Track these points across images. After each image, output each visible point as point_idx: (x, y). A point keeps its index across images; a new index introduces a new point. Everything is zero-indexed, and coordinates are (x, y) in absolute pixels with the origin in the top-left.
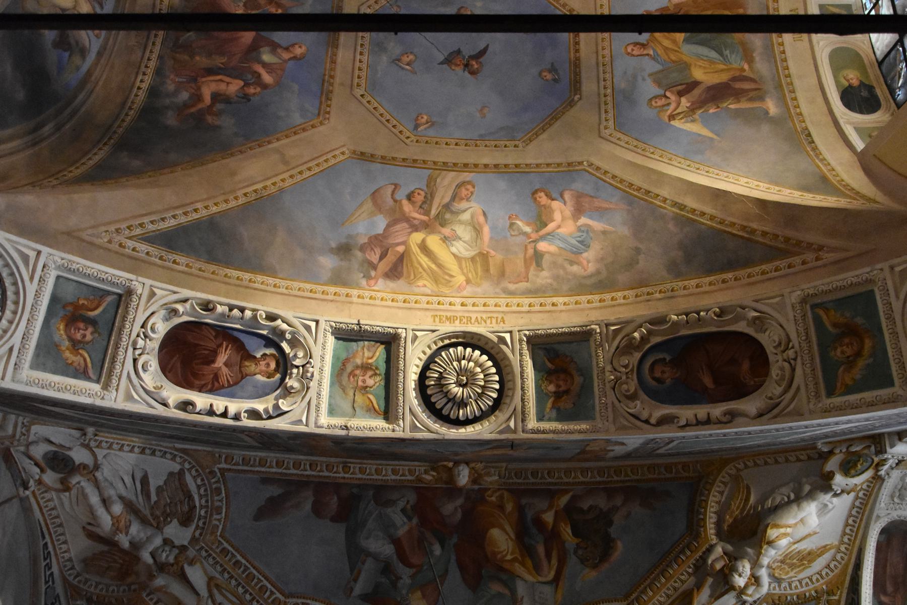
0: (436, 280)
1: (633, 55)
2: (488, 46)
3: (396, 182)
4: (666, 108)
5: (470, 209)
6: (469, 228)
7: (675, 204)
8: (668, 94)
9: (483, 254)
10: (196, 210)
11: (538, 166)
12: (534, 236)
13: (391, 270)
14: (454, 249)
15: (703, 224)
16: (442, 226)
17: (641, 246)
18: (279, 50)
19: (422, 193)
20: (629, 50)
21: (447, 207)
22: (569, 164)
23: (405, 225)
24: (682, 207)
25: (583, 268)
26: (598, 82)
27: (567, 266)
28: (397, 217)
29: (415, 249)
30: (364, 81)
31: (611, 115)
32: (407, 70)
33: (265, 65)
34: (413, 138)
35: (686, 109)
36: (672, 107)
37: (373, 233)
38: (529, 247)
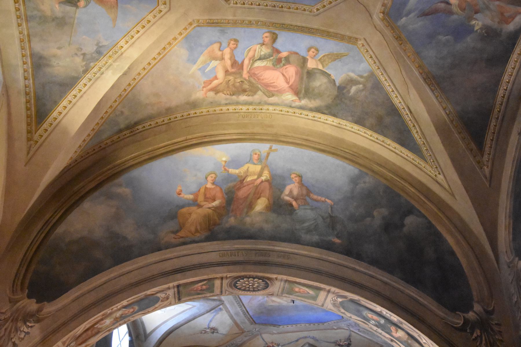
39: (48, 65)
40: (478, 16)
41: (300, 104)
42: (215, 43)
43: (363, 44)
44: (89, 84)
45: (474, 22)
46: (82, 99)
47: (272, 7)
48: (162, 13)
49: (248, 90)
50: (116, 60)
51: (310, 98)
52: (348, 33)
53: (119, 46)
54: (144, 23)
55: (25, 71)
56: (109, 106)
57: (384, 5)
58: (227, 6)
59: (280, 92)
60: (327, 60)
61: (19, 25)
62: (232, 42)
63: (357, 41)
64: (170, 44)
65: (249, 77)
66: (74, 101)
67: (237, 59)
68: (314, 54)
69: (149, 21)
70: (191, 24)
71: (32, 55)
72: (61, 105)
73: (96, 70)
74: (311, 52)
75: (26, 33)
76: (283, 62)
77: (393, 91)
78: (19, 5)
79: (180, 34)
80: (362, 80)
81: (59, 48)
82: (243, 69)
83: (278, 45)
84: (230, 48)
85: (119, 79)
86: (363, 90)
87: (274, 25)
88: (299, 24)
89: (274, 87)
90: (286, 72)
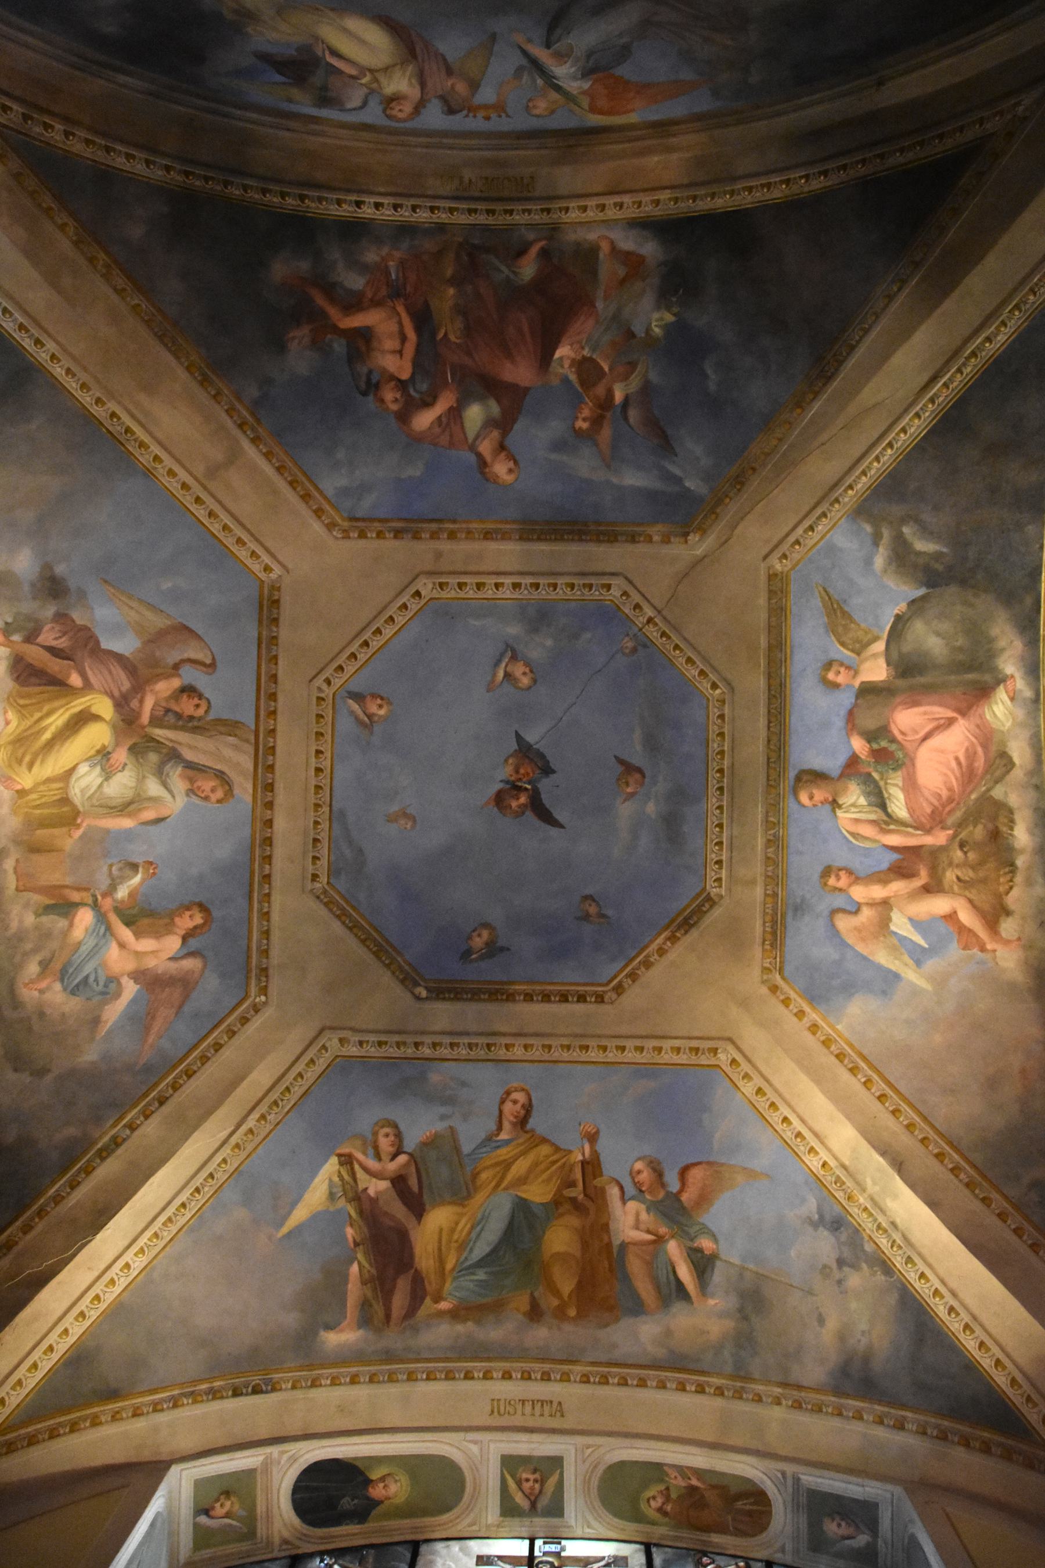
0: (20, 741)
1: (503, 1102)
2: (562, 826)
3: (218, 664)
4: (371, 1151)
5: (169, 795)
6: (129, 794)
7: (116, 1143)
8: (402, 1159)
9: (75, 819)
10: (38, 342)
11: (266, 915)
12: (107, 904)
13: (30, 666)
14: (83, 768)
15: (53, 1182)
16: (130, 749)
17: (49, 1078)
18: (496, 434)
19: (201, 712)
20: (515, 1096)
21: (173, 755)
22: (264, 971)
23: (126, 685)
24: (104, 1154)
25: (32, 981)
26: (451, 1033)
27: (38, 958)
28: (139, 673)
29: (78, 704)
30: (453, 594)
31: (373, 1051)
32: (494, 675)
33: (455, 413)
34: (328, 692)
35: (361, 1186)
36: (372, 1164)
37: (98, 632)
38: (84, 894)
39: (866, 1359)
40: (639, 329)
41: (1018, 676)
42: (833, 926)
43: (780, 559)
44: (922, 1267)
45: (657, 330)
46: (961, 1295)
47: (722, 794)
48: (739, 1058)
49: (990, 826)
50: (858, 1183)
51: (992, 655)
52: (762, 601)
53: (821, 1172)
54: (762, 1104)
55: (880, 1422)
56: (999, 1223)
57: (666, 540)
58: (726, 901)
59: (986, 736)
60: (850, 635)
61: (758, 1399)
62: (832, 881)
63: (776, 575)
64: (827, 1043)
65: (943, 828)
66: (965, 1317)
67: (885, 866)
68: (842, 670)
69: (759, 1091)
70: (774, 989)
71: (838, 1391)
72: (977, 1354)
73: (884, 1241)
74: (840, 679)
75: (778, 1390)
76: (884, 744)
77: (890, 445)
78: (710, 1386)
79: (800, 1014)
80: (886, 533)
81: (821, 1320)
82: (921, 847)
83: (833, 765)
84: (850, 885)
85: (912, 1186)
86: (917, 521)
87: (772, 783)
88: (762, 722)
89: (971, 755)
90: (916, 732)
